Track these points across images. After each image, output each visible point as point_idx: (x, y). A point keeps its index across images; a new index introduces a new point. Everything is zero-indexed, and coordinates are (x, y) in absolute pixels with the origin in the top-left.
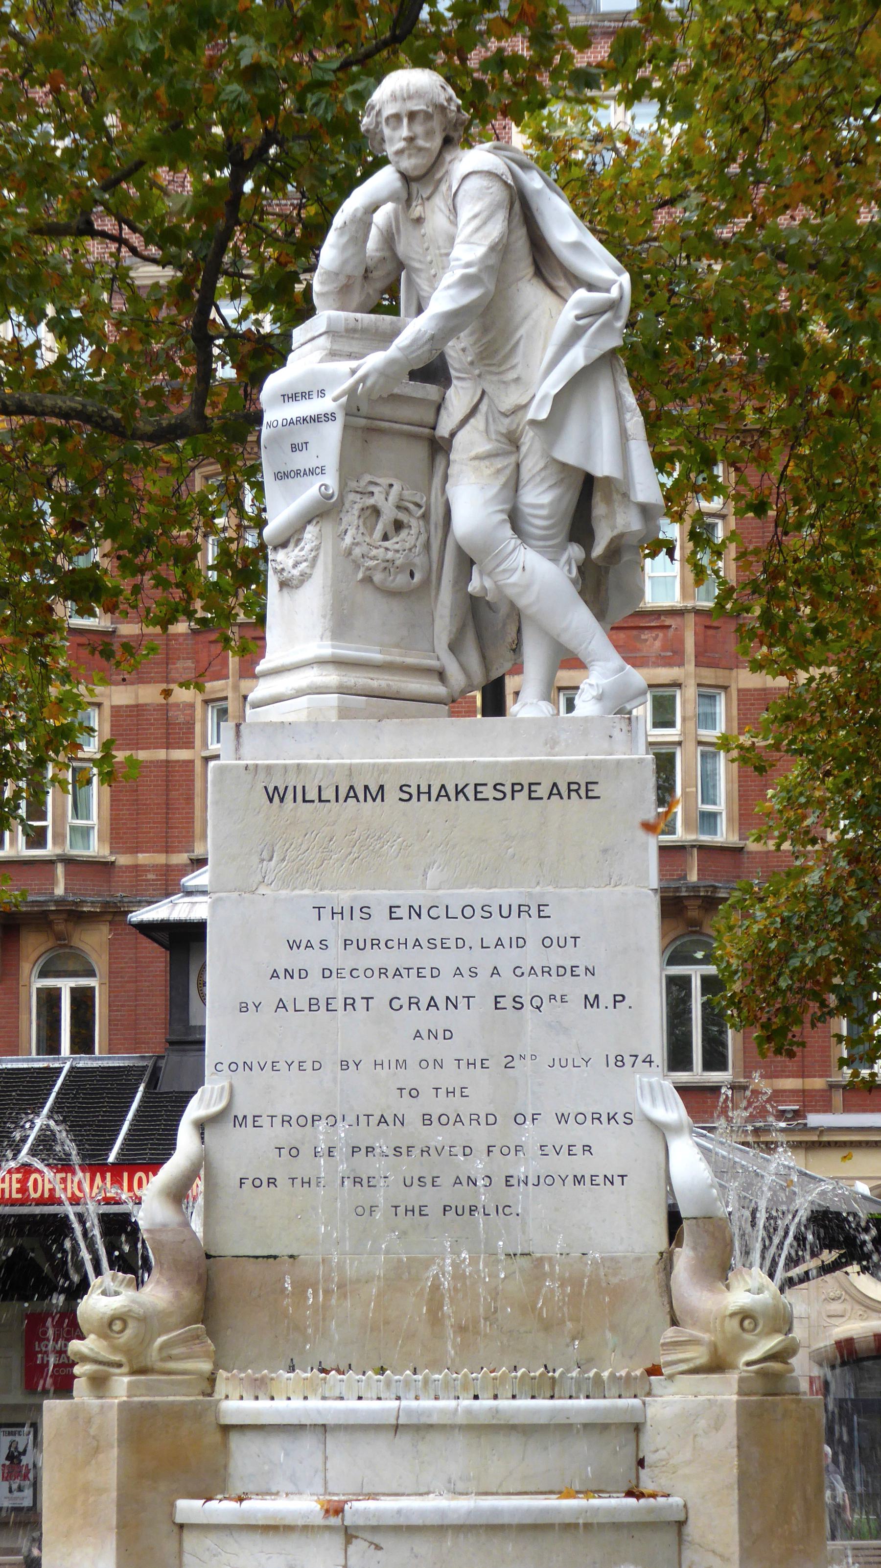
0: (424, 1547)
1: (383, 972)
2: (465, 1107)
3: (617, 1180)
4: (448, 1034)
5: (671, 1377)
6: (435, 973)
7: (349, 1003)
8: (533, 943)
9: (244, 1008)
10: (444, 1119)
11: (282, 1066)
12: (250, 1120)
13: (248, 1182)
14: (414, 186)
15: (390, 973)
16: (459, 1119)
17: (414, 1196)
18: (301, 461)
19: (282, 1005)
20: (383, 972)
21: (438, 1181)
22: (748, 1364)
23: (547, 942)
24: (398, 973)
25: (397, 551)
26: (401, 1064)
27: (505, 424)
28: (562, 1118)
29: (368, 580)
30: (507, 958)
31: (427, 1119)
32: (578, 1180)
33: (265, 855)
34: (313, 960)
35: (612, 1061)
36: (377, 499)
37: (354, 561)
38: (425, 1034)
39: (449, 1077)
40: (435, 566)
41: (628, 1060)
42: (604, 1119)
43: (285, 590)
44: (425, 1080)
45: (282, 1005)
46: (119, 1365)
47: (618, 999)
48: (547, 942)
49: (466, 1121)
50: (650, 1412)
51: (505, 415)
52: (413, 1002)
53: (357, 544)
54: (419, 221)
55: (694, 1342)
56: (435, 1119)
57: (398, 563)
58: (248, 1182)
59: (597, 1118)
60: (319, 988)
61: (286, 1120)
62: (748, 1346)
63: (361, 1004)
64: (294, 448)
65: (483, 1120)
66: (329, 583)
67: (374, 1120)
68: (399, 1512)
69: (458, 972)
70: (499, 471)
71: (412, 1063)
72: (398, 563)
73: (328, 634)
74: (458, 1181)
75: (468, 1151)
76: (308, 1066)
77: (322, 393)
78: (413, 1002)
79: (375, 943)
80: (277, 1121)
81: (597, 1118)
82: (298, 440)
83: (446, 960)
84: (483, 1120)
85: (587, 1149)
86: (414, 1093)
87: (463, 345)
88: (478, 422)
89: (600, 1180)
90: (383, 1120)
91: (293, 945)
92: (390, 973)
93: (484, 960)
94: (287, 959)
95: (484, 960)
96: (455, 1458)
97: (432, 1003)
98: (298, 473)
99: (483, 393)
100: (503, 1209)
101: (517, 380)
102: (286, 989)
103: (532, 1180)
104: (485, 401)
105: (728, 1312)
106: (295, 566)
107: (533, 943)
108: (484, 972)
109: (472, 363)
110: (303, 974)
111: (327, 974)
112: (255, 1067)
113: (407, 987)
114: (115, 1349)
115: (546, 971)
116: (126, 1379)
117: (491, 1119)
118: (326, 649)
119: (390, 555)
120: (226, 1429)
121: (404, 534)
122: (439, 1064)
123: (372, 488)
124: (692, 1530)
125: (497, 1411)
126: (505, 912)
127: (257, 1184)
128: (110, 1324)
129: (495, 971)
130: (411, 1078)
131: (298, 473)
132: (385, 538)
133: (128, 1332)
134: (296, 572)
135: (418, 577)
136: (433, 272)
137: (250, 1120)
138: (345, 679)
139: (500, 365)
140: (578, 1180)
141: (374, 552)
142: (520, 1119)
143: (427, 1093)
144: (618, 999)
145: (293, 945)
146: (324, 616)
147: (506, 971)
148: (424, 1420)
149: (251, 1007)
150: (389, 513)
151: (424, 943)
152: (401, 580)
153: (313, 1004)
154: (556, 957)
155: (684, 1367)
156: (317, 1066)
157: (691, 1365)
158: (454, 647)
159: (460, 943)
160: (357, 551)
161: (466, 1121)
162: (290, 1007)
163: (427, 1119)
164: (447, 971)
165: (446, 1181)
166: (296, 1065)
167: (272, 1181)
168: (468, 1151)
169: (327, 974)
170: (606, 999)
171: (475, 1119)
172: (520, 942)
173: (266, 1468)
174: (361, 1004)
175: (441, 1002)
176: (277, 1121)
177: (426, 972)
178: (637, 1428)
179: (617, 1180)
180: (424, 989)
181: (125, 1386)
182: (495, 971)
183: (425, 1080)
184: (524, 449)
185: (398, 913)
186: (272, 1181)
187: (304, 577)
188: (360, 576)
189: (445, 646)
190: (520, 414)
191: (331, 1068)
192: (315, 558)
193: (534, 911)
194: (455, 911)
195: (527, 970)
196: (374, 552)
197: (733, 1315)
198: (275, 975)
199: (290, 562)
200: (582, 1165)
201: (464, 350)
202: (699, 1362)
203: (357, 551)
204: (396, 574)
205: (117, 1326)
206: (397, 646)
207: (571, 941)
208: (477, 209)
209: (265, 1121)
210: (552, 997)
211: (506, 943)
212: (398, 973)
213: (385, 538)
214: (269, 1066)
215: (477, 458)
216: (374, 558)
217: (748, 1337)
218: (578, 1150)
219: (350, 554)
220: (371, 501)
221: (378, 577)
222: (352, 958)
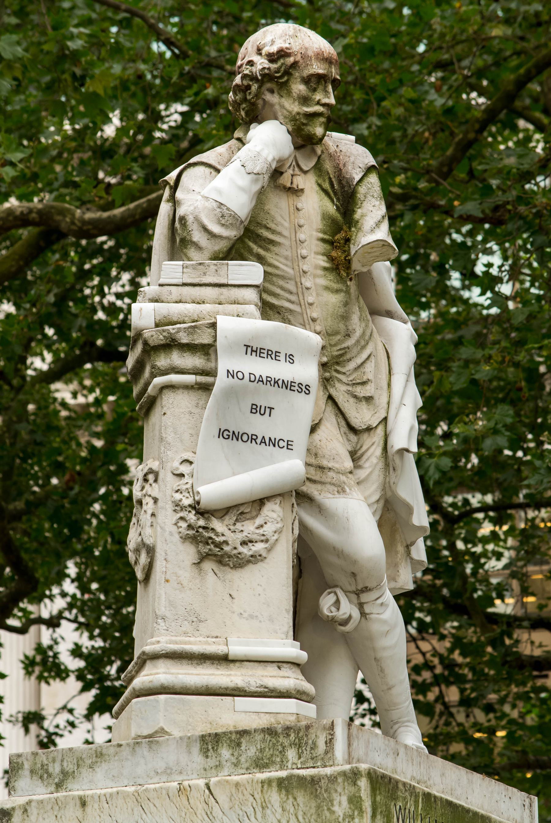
18: (259, 426)
43: (208, 566)
64: (255, 409)
77: (290, 358)
82: (262, 402)
98: (253, 438)
106: (244, 543)
131: (253, 438)
187: (255, 559)
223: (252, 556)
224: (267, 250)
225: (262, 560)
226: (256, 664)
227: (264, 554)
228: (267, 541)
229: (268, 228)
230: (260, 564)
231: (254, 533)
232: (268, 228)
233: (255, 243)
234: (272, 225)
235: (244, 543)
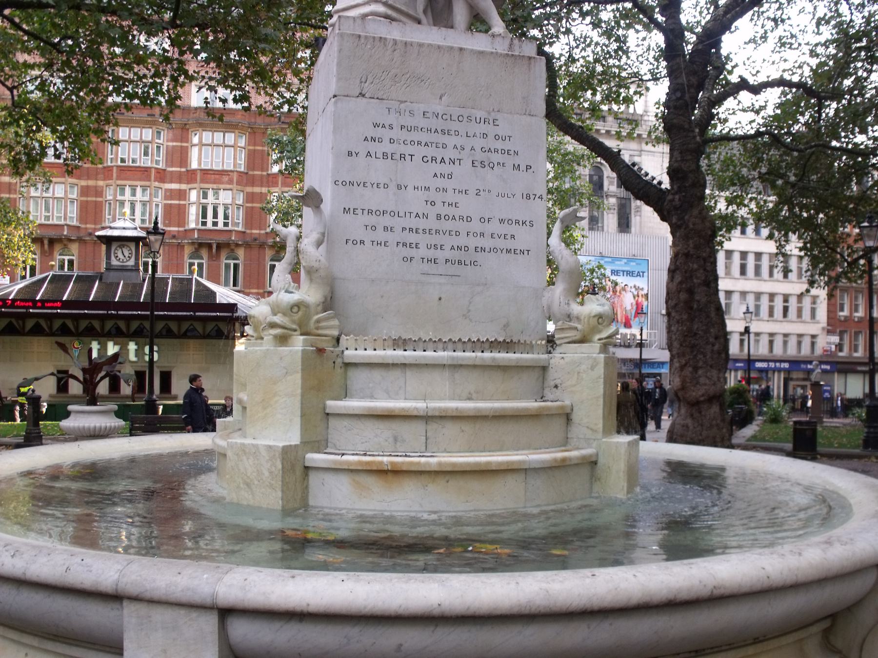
0: (467, 427)
1: (419, 143)
2: (457, 212)
3: (526, 252)
4: (450, 177)
5: (561, 345)
6: (445, 146)
7: (402, 157)
8: (491, 136)
9: (350, 154)
10: (447, 217)
11: (368, 184)
12: (352, 210)
13: (350, 242)
15: (423, 144)
16: (454, 218)
17: (432, 253)
19: (369, 154)
20: (419, 143)
21: (444, 247)
22: (600, 339)
23: (497, 137)
24: (426, 144)
26: (427, 189)
28: (502, 221)
30: (478, 143)
31: (439, 217)
32: (509, 251)
33: (363, 80)
34: (386, 134)
35: (525, 196)
38: (439, 175)
39: (450, 197)
41: (532, 197)
42: (521, 223)
44: (438, 198)
45: (369, 154)
46: (295, 330)
47: (529, 167)
48: (497, 137)
49: (457, 219)
50: (552, 361)
52: (434, 159)
55: (576, 328)
56: (443, 217)
58: (350, 242)
59: (517, 222)
60: (388, 148)
61: (370, 212)
62: (600, 332)
63: (408, 158)
65: (465, 219)
67: (413, 215)
68: (457, 409)
69: (455, 147)
71: (432, 189)
74: (452, 248)
75: (458, 234)
76: (382, 186)
78: (434, 159)
79: (416, 128)
80: (366, 212)
81: (517, 222)
83: (451, 141)
84: (465, 219)
85: (513, 237)
86: (433, 204)
89: (518, 252)
90: (417, 215)
91: (376, 125)
92: (423, 144)
93: (468, 143)
94: (371, 132)
95: (468, 143)
96: (441, 381)
97: (443, 160)
100: (474, 263)
102: (372, 147)
103: (487, 250)
105: (593, 314)
107: (491, 136)
108: (468, 149)
110: (380, 140)
111: (392, 141)
112: (355, 184)
113: (430, 152)
114: (294, 322)
115: (496, 151)
116: (302, 337)
117: (469, 219)
120: (347, 365)
122: (445, 190)
124: (575, 417)
125: (494, 359)
126: (478, 121)
127: (354, 242)
128: (292, 308)
129: (472, 149)
130: (432, 195)
133: (300, 313)
137: (352, 210)
140: (509, 251)
142: (482, 220)
143: (439, 204)
144: (529, 167)
145: (376, 125)
147: (478, 149)
148: (460, 362)
149: (354, 154)
151: (439, 131)
153: (385, 155)
154: (499, 145)
155: (567, 340)
156: (386, 186)
157: (570, 340)
158: (425, 12)
159: (457, 133)
161: (457, 219)
162: (374, 156)
163: (439, 217)
164: (450, 146)
165: (447, 247)
166: (375, 185)
167: (362, 242)
168: (458, 234)
169: (392, 141)
170: (523, 167)
171: (461, 218)
172: (485, 136)
173: (371, 385)
174: (408, 158)
175: (447, 161)
176: (366, 212)
177: (441, 146)
178: (544, 369)
179: (526, 252)
180: (439, 154)
181: (301, 341)
182: (472, 149)
183: (438, 198)
185: (428, 115)
186: (362, 242)
191: (393, 187)
193: (491, 122)
194: (455, 117)
195: (487, 149)
197: (594, 316)
198: (366, 139)
200: (510, 244)
202: (574, 338)
205: (295, 309)
207: (508, 138)
209: (359, 212)
210: (499, 164)
211: (478, 135)
212: (426, 144)
214: (362, 184)
217: (600, 326)
218: (508, 237)
222: (404, 135)
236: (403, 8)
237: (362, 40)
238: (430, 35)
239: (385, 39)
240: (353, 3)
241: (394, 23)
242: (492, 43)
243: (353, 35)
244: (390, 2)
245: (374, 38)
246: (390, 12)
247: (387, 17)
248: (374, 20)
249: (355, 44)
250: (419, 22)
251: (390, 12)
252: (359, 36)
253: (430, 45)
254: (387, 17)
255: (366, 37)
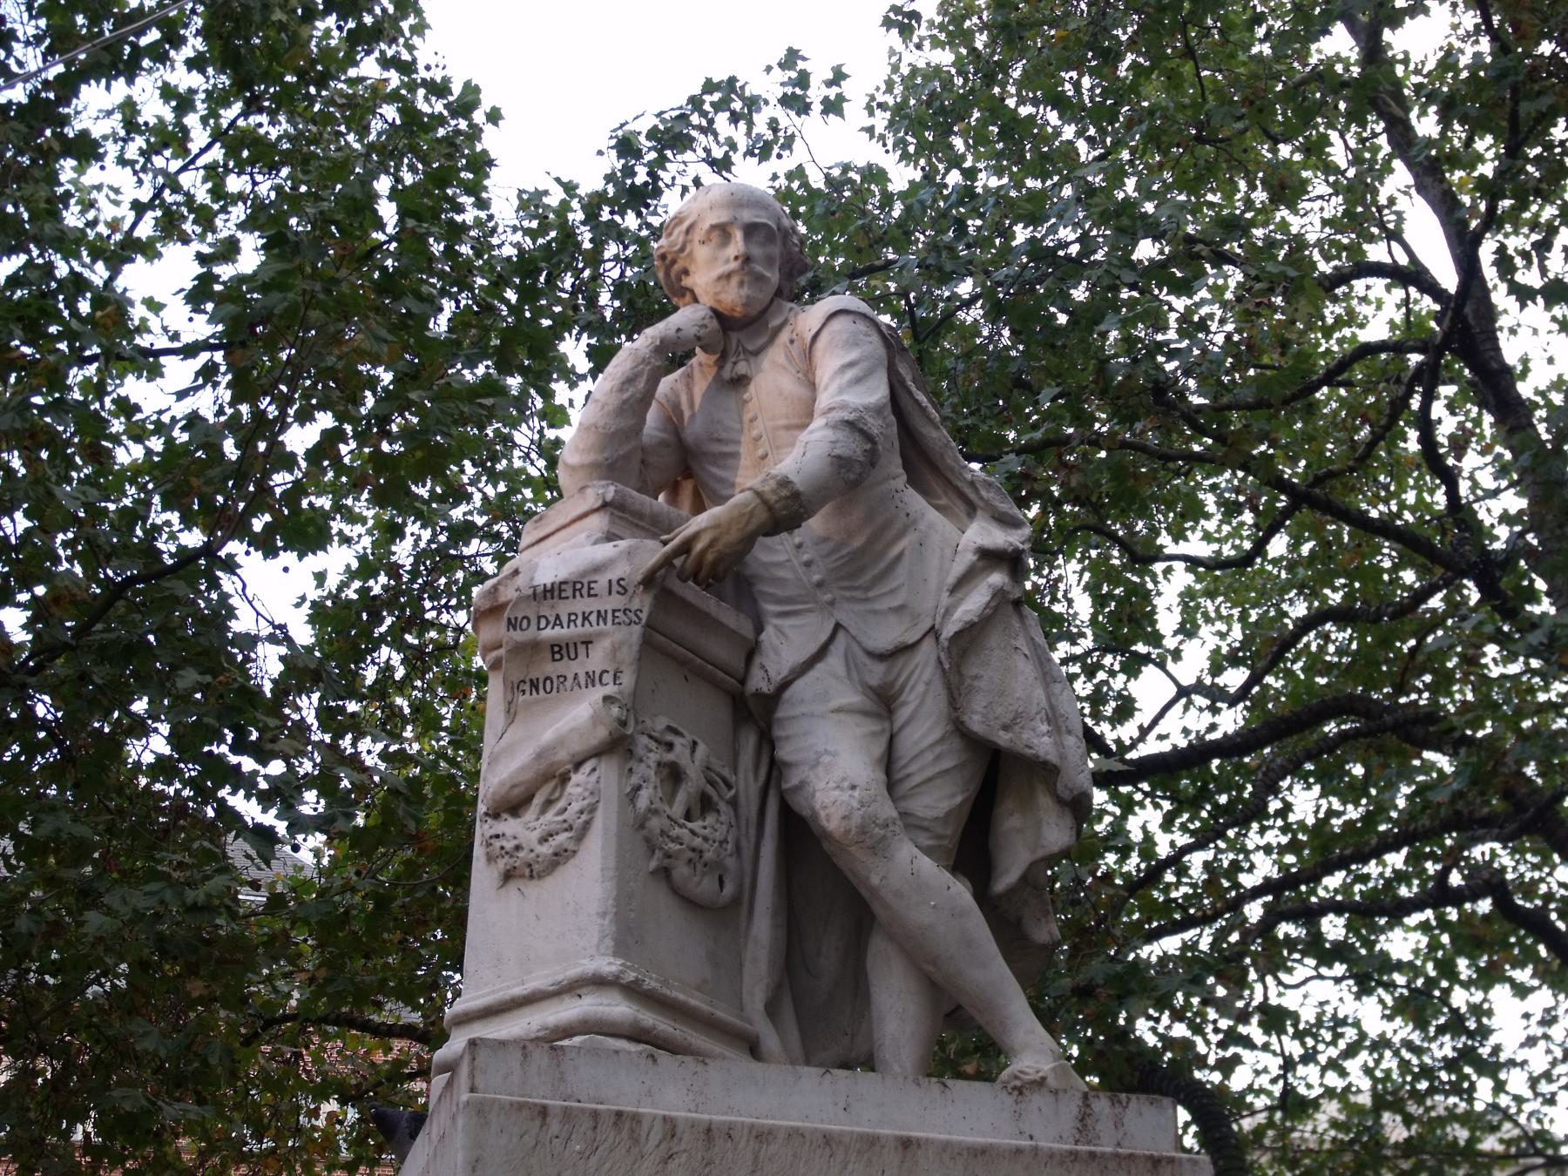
14: (734, 336)
25: (706, 839)
27: (876, 673)
29: (664, 873)
36: (680, 754)
37: (647, 840)
40: (747, 881)
43: (512, 886)
51: (882, 657)
53: (656, 812)
54: (740, 382)
57: (708, 855)
66: (612, 863)
70: (874, 734)
72: (708, 855)
73: (609, 942)
87: (806, 557)
88: (835, 661)
99: (838, 626)
101: (900, 609)
104: (841, 636)
106: (543, 840)
109: (820, 585)
118: (608, 965)
119: (698, 842)
121: (710, 819)
123: (670, 737)
132: (688, 816)
134: (546, 850)
135: (729, 889)
136: (760, 452)
138: (640, 1016)
139: (867, 589)
141: (677, 831)
146: (603, 915)
150: (695, 778)
152: (704, 886)
158: (772, 1009)
160: (655, 823)
184: (903, 714)
187: (560, 857)
188: (653, 864)
189: (760, 1006)
190: (901, 661)
192: (587, 825)
196: (677, 831)
199: (536, 835)
201: (808, 564)
203: (655, 823)
204: (704, 874)
206: (698, 989)
208: (853, 355)
213: (688, 816)
215: (839, 710)
216: (677, 840)
219: (642, 826)
220: (670, 757)
221: (681, 871)
223: (556, 854)
224: (724, 467)
225: (568, 859)
226: (555, 1001)
227: (571, 847)
228: (570, 828)
229: (719, 441)
230: (572, 861)
231: (551, 823)
232: (719, 441)
233: (715, 464)
234: (724, 435)
235: (543, 840)
236: (696, 1001)
237: (555, 1126)
238: (797, 1099)
239: (636, 1118)
240: (518, 991)
241: (664, 1057)
242: (1018, 1115)
243: (521, 1106)
244: (651, 983)
245: (595, 1114)
246: (649, 1018)
247: (637, 1035)
248: (595, 1052)
249: (529, 1140)
250: (754, 1049)
251: (649, 1018)
252: (544, 1112)
253: (794, 1134)
254: (637, 1035)
255: (567, 1113)
